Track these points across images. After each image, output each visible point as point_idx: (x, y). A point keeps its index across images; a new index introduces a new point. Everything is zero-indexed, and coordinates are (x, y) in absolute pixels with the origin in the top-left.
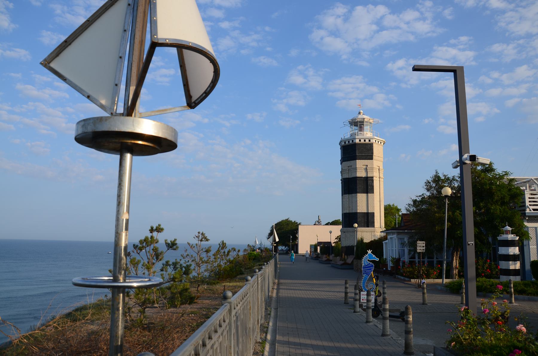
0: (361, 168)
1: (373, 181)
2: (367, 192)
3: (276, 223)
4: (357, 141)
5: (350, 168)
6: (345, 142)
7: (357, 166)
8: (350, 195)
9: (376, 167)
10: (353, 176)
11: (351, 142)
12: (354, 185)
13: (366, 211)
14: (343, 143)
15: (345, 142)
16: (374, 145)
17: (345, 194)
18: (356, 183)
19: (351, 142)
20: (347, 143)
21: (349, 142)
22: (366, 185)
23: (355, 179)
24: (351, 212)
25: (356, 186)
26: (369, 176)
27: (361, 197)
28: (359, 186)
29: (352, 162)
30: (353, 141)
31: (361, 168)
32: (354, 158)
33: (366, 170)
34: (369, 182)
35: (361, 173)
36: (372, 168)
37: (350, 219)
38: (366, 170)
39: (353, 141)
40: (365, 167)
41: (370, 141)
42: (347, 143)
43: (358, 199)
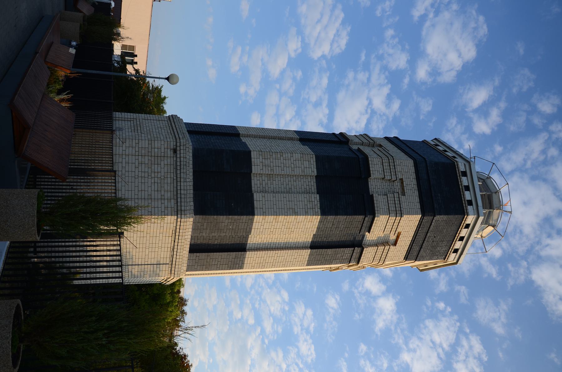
4: (470, 219)
5: (397, 184)
6: (464, 174)
8: (312, 184)
10: (379, 201)
13: (253, 239)
14: (462, 167)
15: (464, 174)
17: (320, 161)
18: (355, 213)
21: (467, 188)
23: (367, 209)
24: (255, 182)
25: (346, 214)
26: (368, 253)
28: (343, 225)
29: (412, 196)
30: (470, 203)
32: (428, 208)
34: (348, 251)
37: (222, 176)
38: (384, 243)
39: (470, 203)
41: (456, 251)
43: (301, 218)
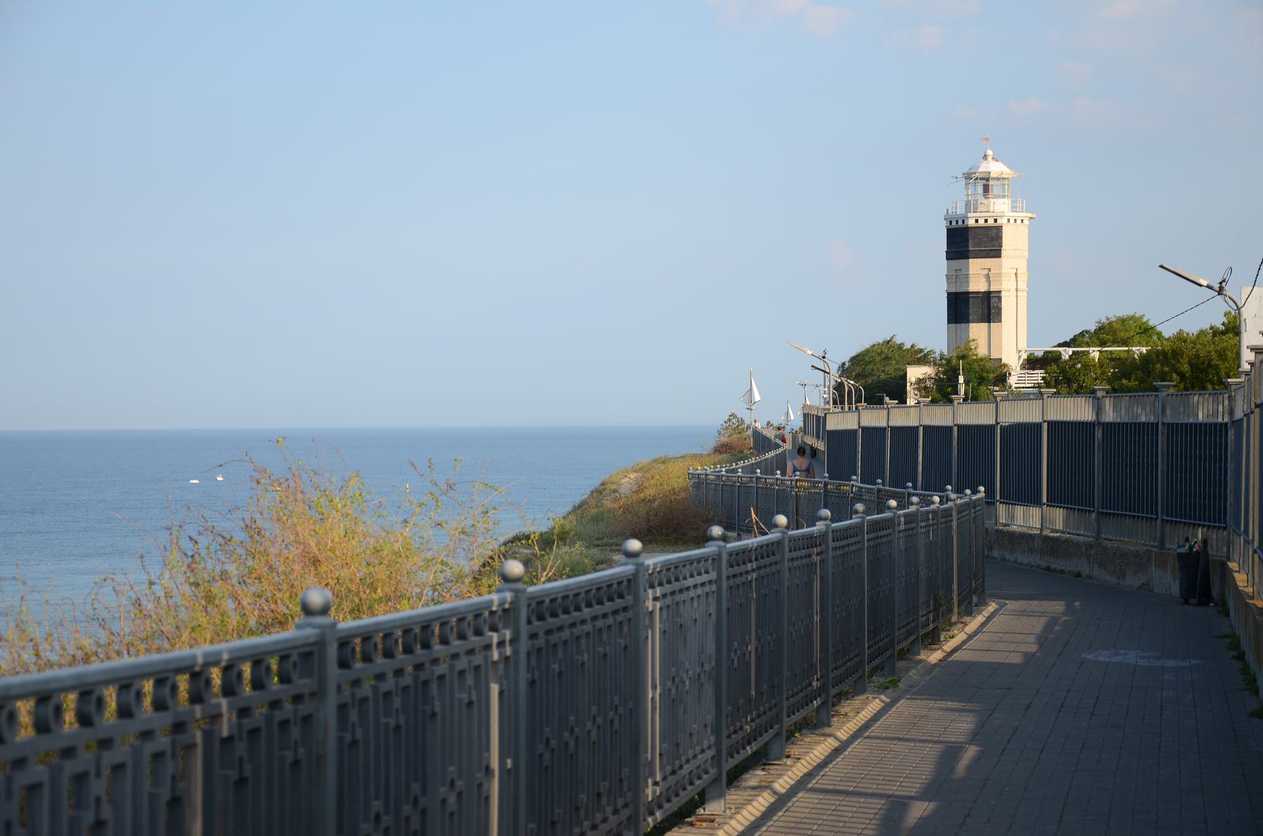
0: (977, 275)
1: (1000, 298)
2: (989, 322)
3: (853, 354)
4: (971, 222)
7: (971, 272)
9: (1008, 273)
11: (960, 223)
12: (968, 307)
16: (1004, 230)
19: (960, 223)
20: (954, 223)
22: (987, 307)
27: (977, 331)
28: (974, 309)
31: (977, 275)
33: (988, 276)
34: (993, 300)
35: (977, 285)
36: (1000, 275)
38: (988, 276)
40: (986, 272)
42: (954, 223)
